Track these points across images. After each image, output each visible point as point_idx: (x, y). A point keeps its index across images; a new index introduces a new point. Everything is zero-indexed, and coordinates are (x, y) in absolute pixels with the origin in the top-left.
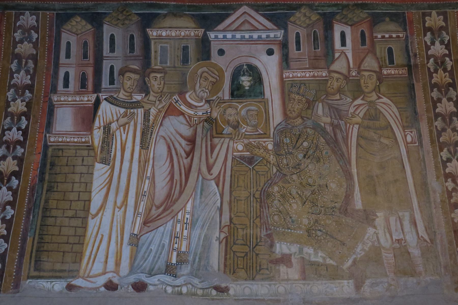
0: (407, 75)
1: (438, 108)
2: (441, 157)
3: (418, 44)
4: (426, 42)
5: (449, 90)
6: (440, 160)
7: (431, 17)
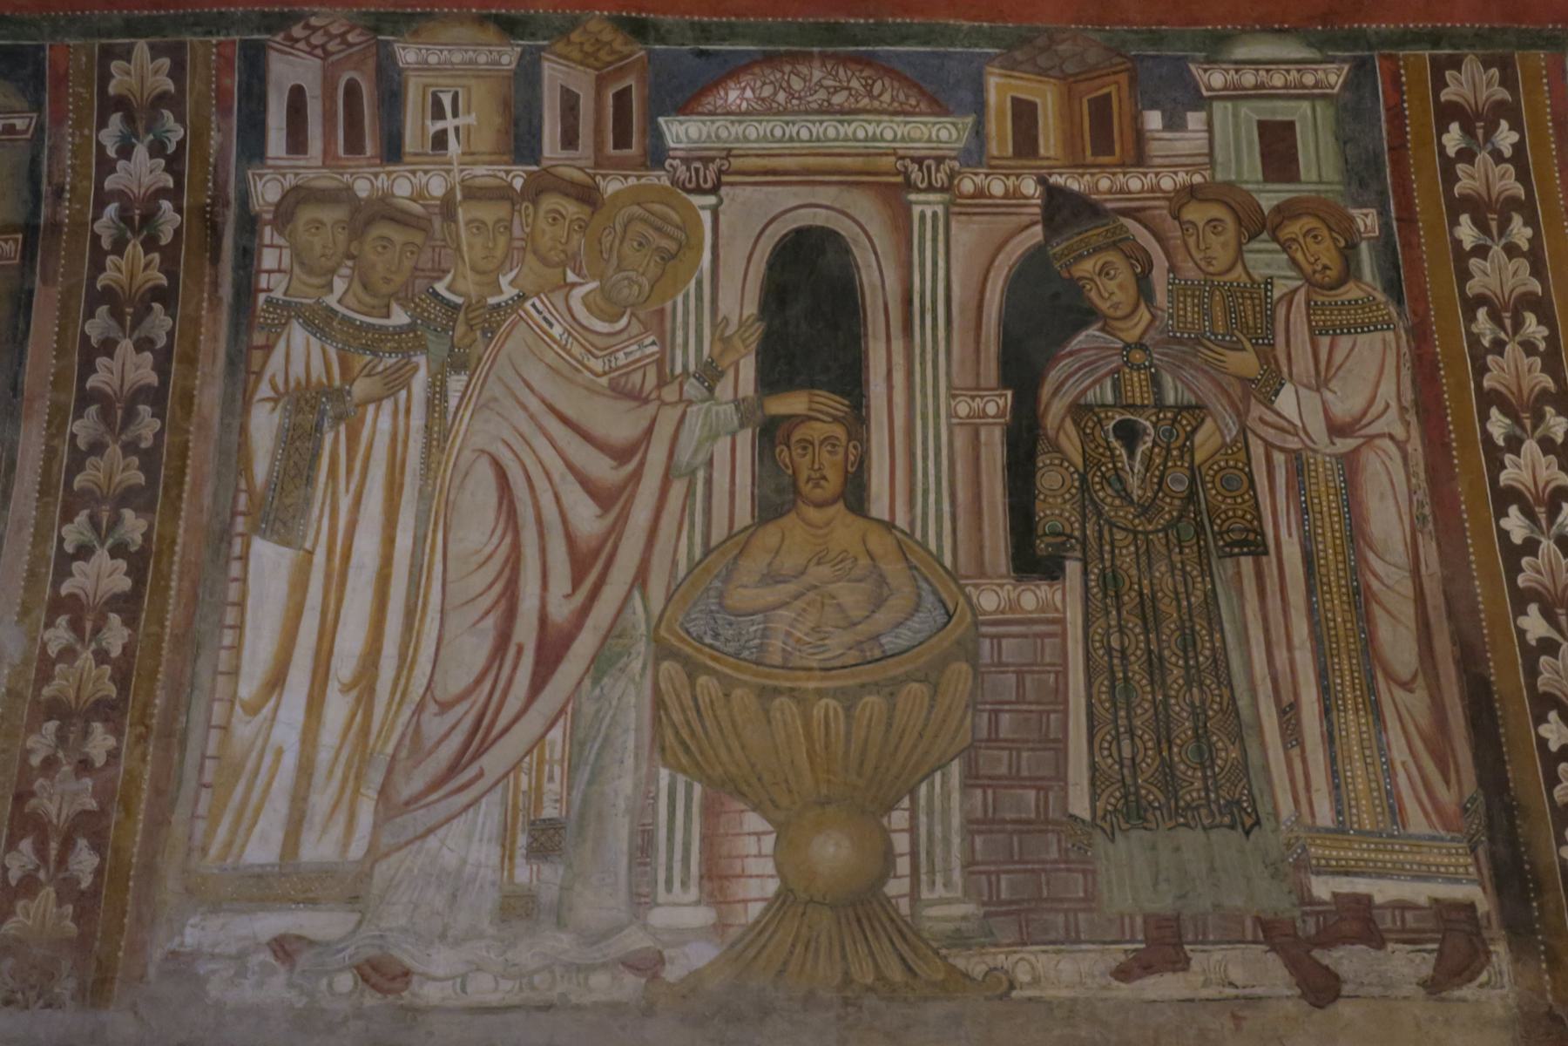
0: (17, 261)
1: (95, 371)
2: (61, 540)
3: (75, 155)
4: (101, 148)
5: (149, 309)
6: (53, 553)
7: (129, 61)
